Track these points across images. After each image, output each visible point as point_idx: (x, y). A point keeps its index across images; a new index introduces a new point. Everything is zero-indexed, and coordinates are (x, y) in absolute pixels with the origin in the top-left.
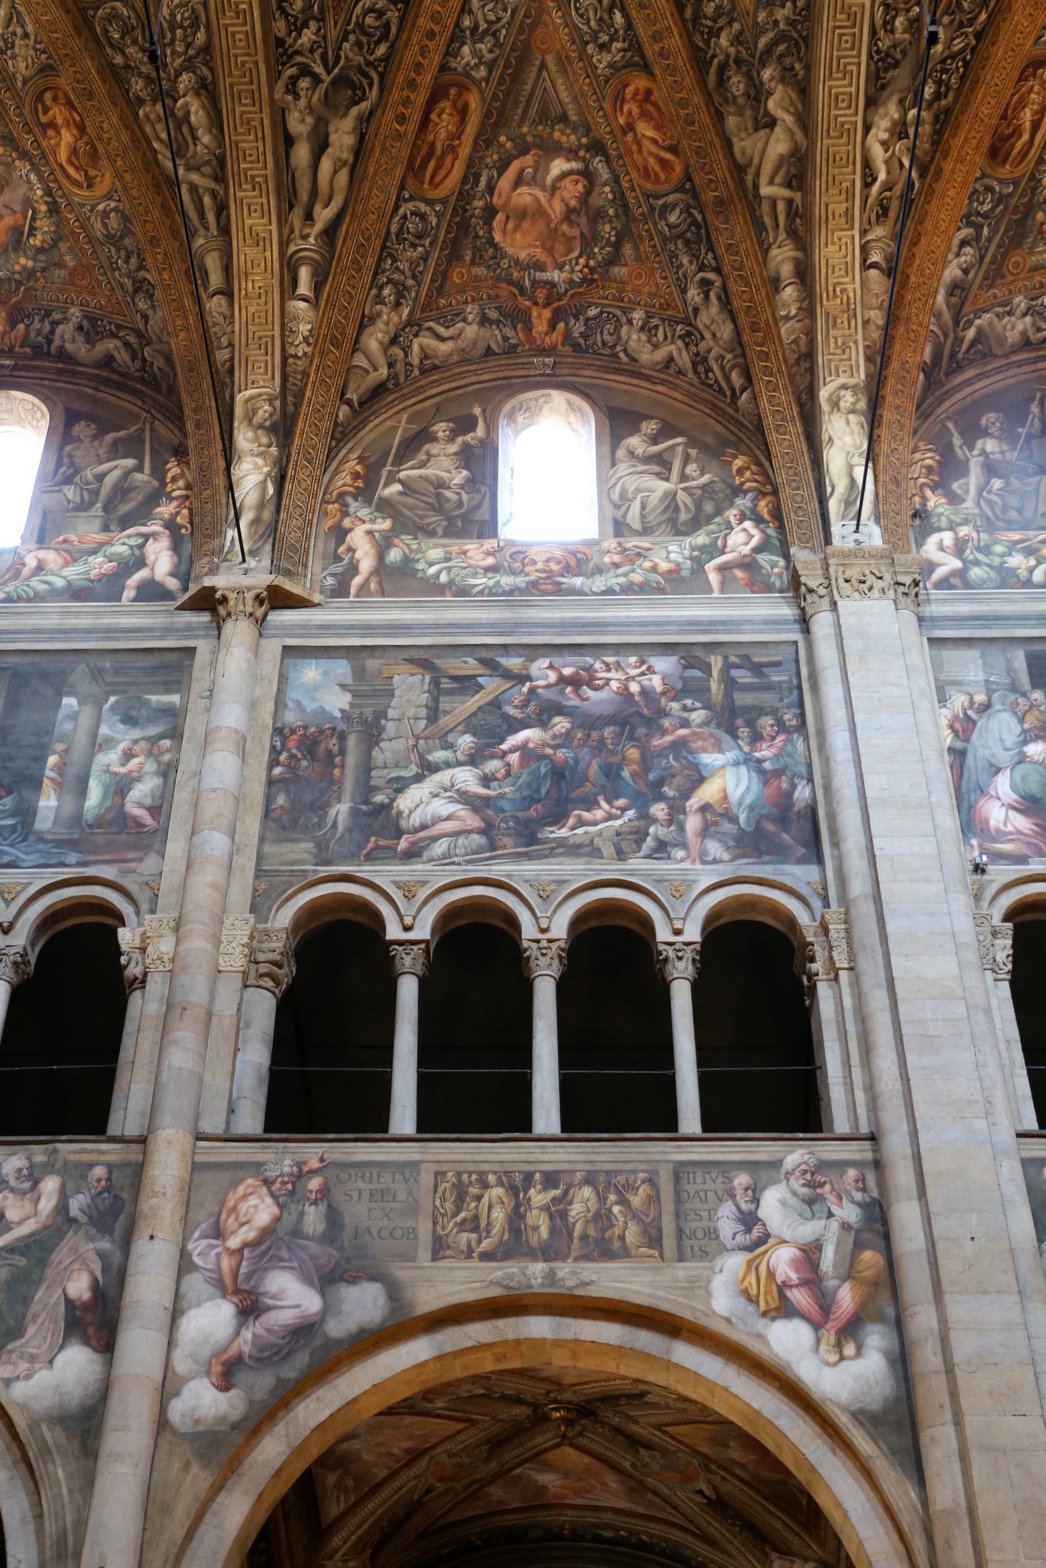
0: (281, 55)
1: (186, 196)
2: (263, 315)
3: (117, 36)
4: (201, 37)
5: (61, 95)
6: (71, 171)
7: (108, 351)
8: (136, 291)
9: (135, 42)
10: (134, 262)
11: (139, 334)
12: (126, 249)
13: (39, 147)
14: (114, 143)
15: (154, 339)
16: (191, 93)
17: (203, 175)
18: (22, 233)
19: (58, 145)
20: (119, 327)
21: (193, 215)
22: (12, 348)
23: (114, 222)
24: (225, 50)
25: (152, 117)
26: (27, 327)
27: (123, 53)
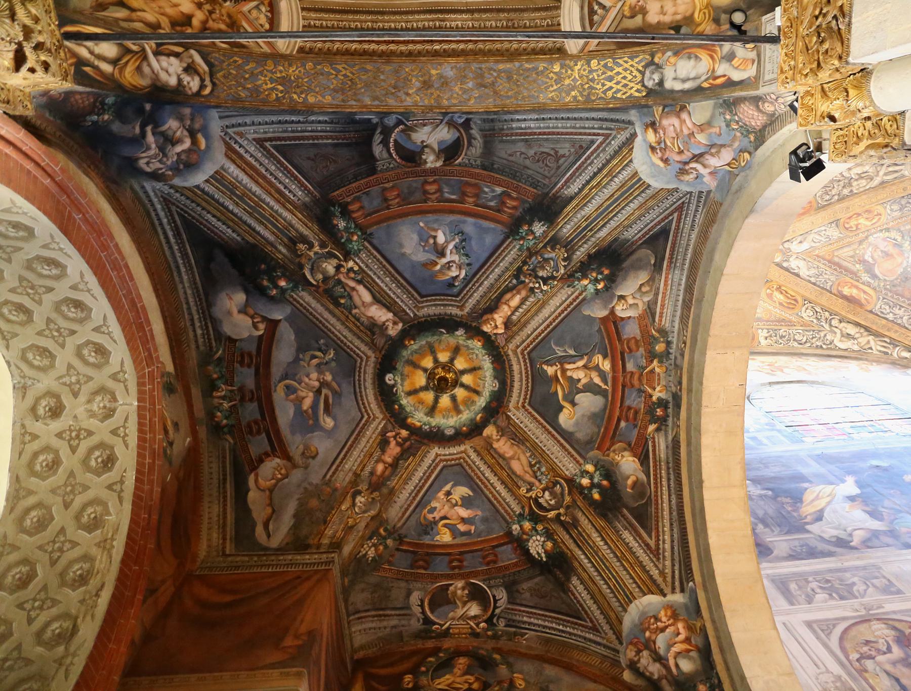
6: (874, 221)
23: (895, 207)
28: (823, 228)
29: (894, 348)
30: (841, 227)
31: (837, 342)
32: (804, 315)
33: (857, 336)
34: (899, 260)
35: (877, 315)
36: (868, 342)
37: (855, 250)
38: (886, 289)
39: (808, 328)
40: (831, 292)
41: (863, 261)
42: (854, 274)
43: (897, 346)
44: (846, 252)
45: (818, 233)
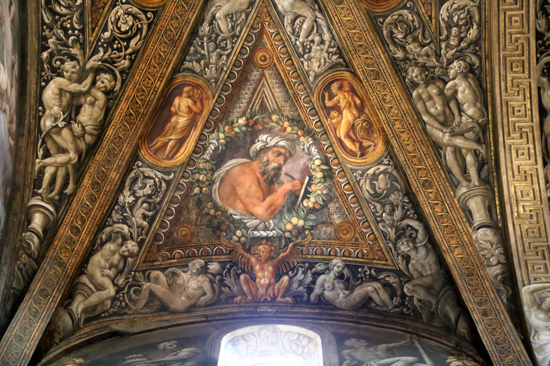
0: (540, 46)
1: (450, 157)
2: (536, 230)
3: (400, 36)
4: (473, 32)
5: (346, 84)
6: (348, 143)
7: (367, 293)
8: (398, 238)
9: (415, 40)
10: (398, 213)
11: (399, 273)
12: (392, 204)
13: (322, 125)
14: (394, 111)
15: (415, 275)
16: (459, 76)
17: (467, 139)
18: (298, 197)
19: (339, 123)
20: (379, 271)
21: (456, 171)
22: (274, 298)
23: (381, 183)
24: (502, 29)
25: (424, 96)
26: (291, 278)
27: (404, 48)
28: (327, 37)
29: (50, 201)
30: (330, 75)
31: (59, 80)
32: (119, 10)
33: (76, 127)
34: (260, 210)
35: (129, 170)
36: (63, 151)
37: (279, 111)
38: (191, 186)
39: (88, 19)
40: (176, 70)
41: (252, 132)
42: (221, 117)
43: (57, 209)
44: (273, 94)
45: (315, 27)
